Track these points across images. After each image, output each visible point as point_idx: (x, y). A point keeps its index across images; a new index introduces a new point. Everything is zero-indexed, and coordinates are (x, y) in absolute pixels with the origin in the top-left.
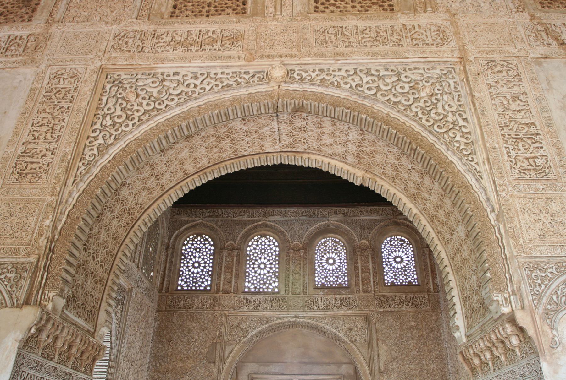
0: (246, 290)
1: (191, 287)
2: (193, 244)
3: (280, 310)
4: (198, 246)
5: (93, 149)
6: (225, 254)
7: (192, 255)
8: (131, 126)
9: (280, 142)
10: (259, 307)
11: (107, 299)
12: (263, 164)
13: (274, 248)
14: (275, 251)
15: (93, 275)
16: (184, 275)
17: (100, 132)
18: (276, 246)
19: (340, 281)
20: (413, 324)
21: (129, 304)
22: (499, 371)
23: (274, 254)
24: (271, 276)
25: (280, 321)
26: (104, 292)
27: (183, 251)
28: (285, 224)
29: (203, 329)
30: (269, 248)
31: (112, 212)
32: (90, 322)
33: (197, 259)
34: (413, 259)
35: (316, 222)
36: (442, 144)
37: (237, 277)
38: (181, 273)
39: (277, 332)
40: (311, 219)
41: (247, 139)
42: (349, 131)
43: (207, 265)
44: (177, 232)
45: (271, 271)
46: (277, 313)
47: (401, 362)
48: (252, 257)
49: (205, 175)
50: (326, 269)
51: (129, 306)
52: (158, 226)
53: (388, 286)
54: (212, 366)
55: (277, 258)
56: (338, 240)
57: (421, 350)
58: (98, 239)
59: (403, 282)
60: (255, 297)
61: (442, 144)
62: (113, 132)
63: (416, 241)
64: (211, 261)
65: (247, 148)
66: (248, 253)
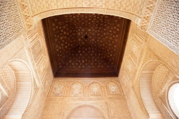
6: (67, 88)
20: (119, 104)
25: (81, 104)
28: (83, 81)
37: (69, 93)
54: (60, 116)
60: (74, 98)
63: (117, 85)
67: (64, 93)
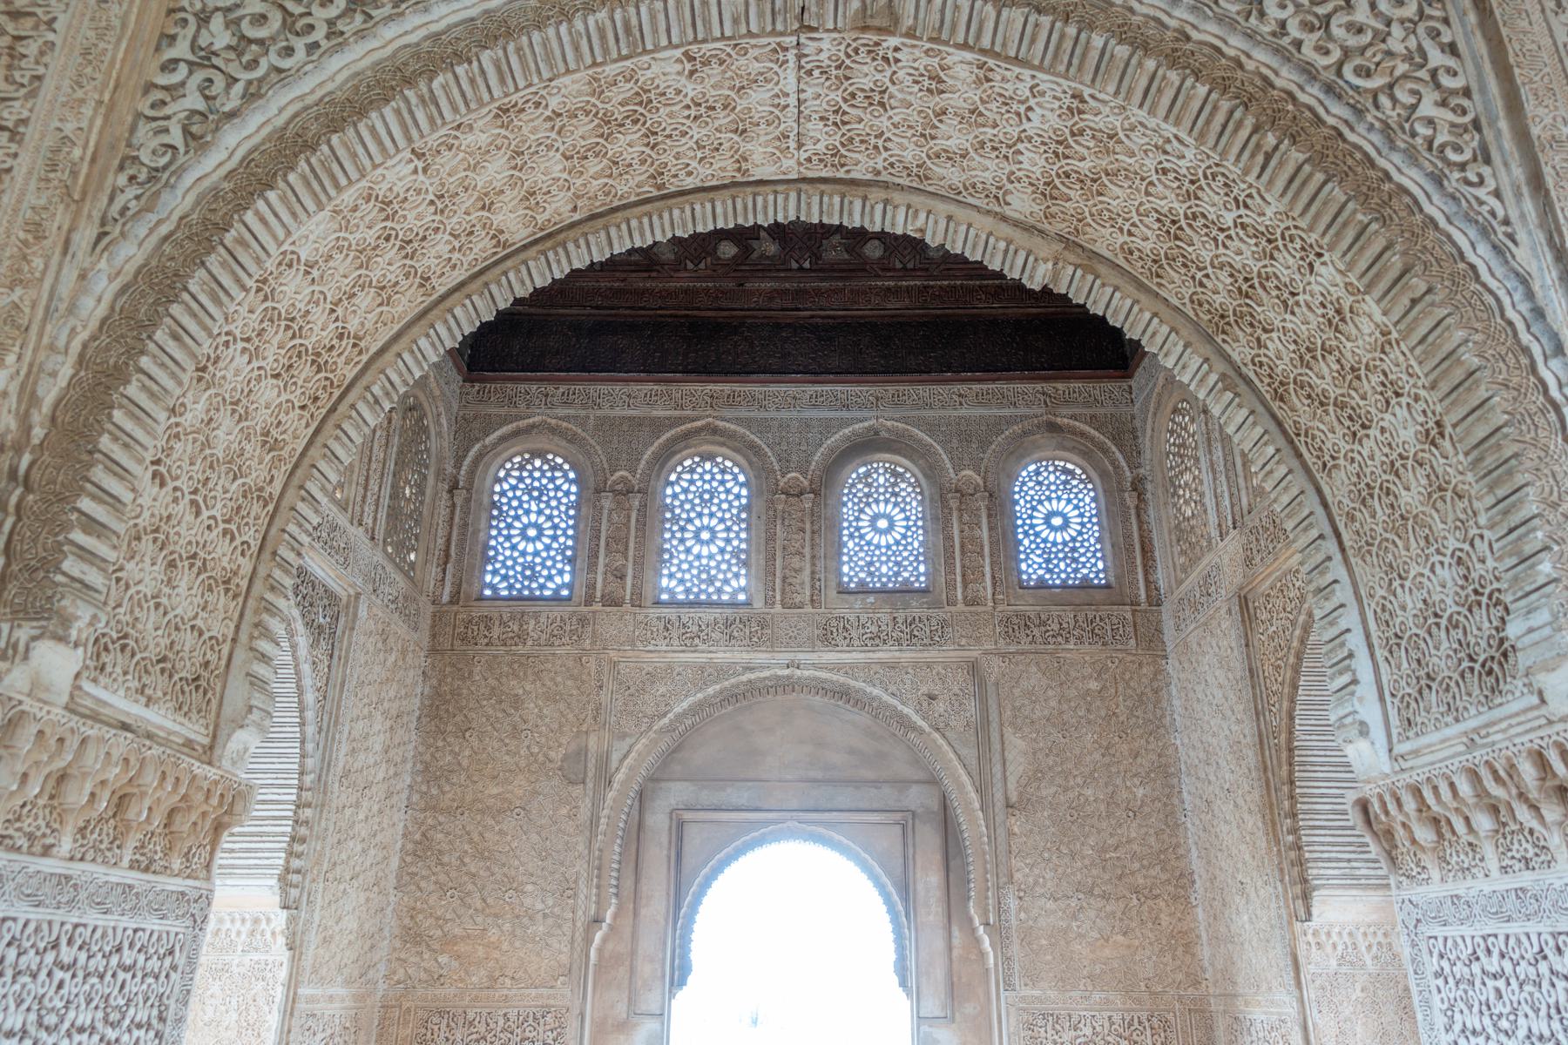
0: (665, 597)
1: (519, 591)
2: (521, 479)
3: (753, 646)
4: (536, 484)
5: (167, 131)
6: (607, 502)
7: (520, 506)
8: (301, 54)
9: (800, 146)
10: (697, 641)
11: (252, 637)
12: (740, 221)
13: (736, 490)
14: (738, 497)
15: (199, 563)
16: (501, 558)
17: (191, 73)
18: (742, 485)
19: (906, 575)
20: (1094, 685)
21: (350, 636)
22: (1528, 875)
23: (736, 503)
24: (728, 562)
25: (753, 676)
26: (242, 615)
27: (496, 498)
28: (763, 427)
29: (552, 698)
30: (721, 489)
31: (255, 354)
32: (194, 716)
33: (533, 517)
34: (1095, 520)
35: (845, 423)
36: (1371, 127)
37: (639, 563)
38: (492, 553)
39: (745, 703)
40: (832, 414)
41: (697, 132)
42: (1032, 102)
43: (559, 532)
44: (477, 447)
45: (729, 549)
46: (745, 655)
47: (1059, 780)
48: (678, 511)
49: (560, 250)
50: (869, 543)
51: (350, 644)
52: (426, 430)
53: (1028, 588)
54: (577, 791)
55: (744, 516)
56: (901, 470)
57: (1112, 751)
58: (207, 444)
59: (1068, 577)
60: (687, 615)
61: (1371, 127)
62: (234, 69)
63: (1103, 475)
64: (571, 522)
65: (694, 164)
66: (668, 501)
67: (592, 566)
